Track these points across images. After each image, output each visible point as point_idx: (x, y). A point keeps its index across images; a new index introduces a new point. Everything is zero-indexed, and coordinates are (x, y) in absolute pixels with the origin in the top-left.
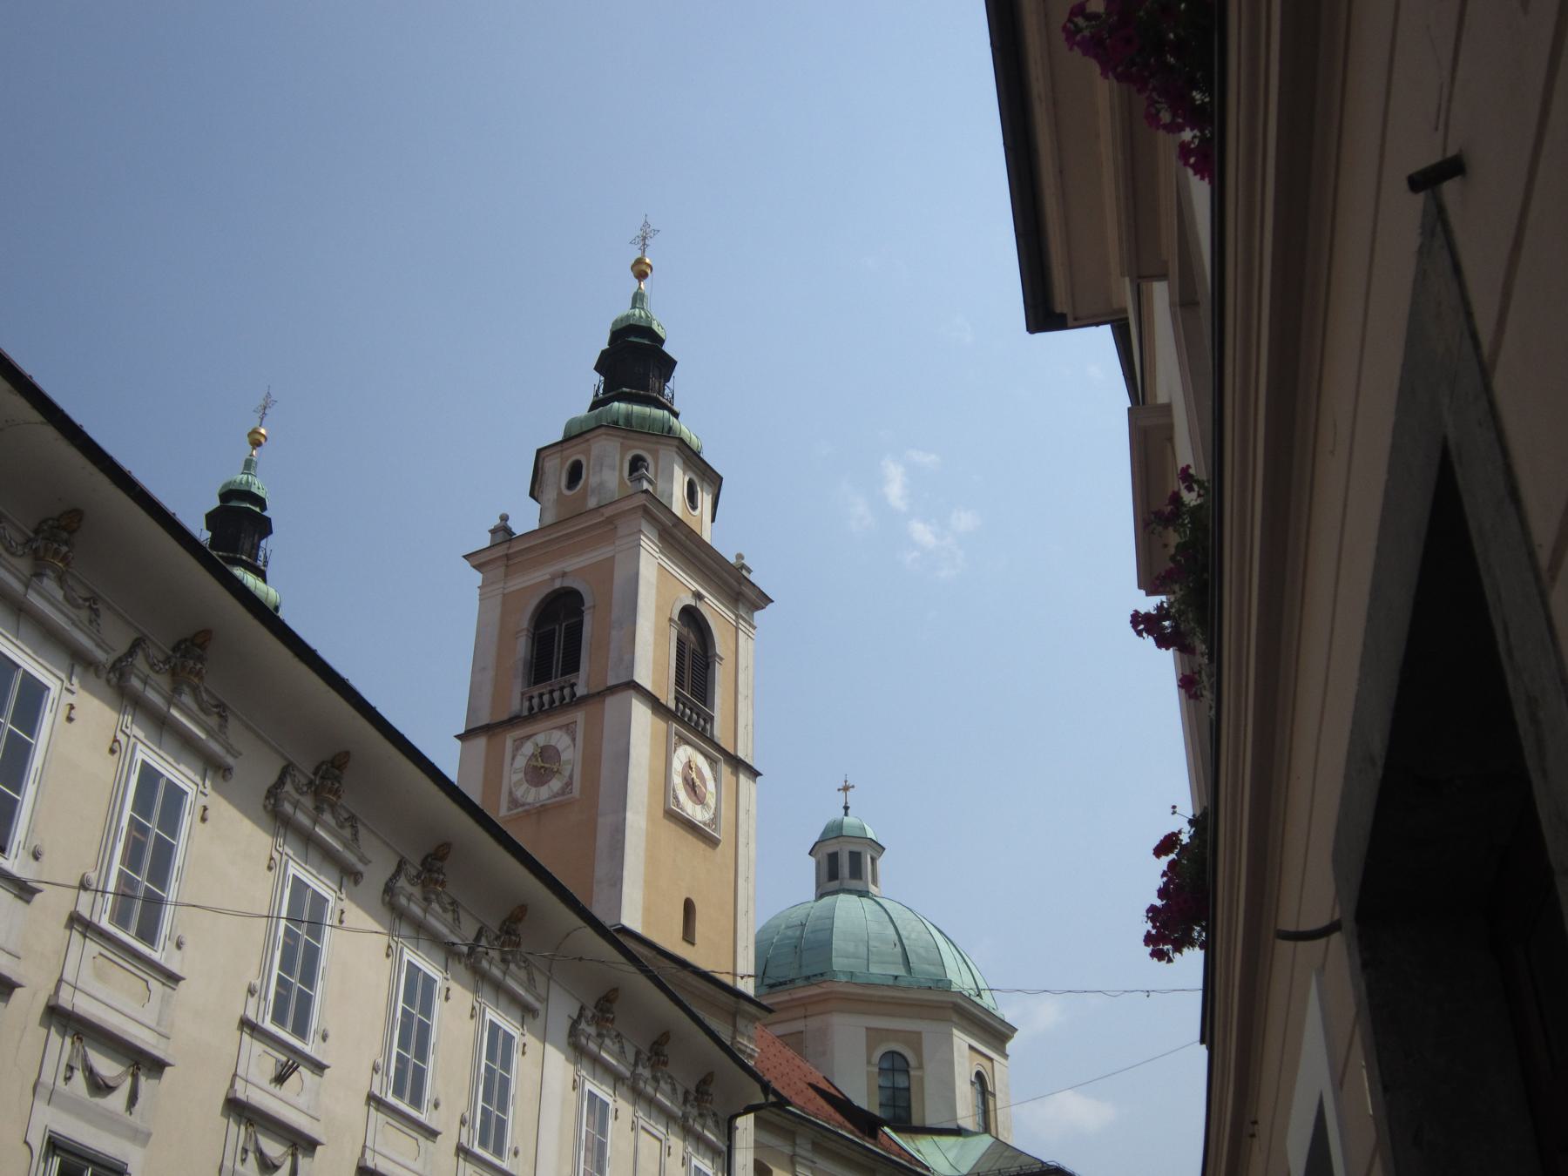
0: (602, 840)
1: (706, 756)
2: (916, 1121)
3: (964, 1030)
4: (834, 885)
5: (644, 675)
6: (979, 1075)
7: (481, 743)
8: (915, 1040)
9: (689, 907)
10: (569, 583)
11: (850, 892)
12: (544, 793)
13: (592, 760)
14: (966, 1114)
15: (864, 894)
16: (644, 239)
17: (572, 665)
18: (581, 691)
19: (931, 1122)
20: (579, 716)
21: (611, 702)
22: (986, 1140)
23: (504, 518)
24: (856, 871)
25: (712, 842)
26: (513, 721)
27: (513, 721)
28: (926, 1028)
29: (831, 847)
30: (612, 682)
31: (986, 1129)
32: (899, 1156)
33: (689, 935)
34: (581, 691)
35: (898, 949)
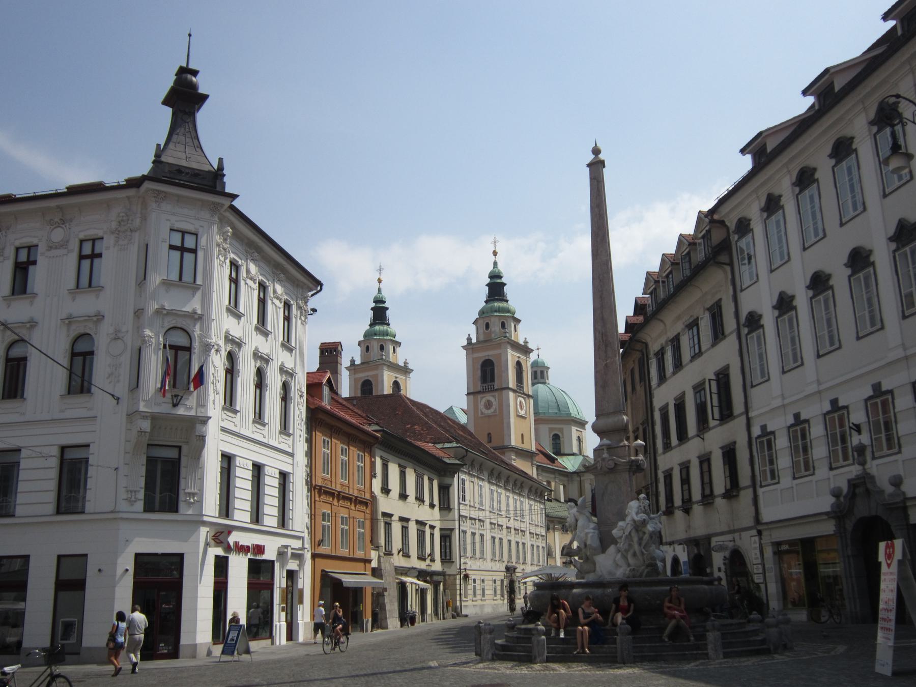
0: (505, 425)
1: (523, 398)
2: (562, 452)
3: (574, 426)
4: (536, 381)
5: (511, 386)
6: (579, 437)
7: (471, 397)
8: (561, 430)
9: (522, 435)
10: (490, 358)
11: (541, 383)
12: (490, 412)
13: (501, 405)
14: (575, 450)
15: (544, 383)
16: (495, 243)
17: (493, 380)
18: (496, 388)
19: (566, 452)
20: (496, 394)
21: (504, 392)
22: (580, 458)
23: (469, 335)
24: (542, 377)
25: (525, 418)
26: (479, 392)
27: (479, 392)
28: (565, 427)
29: (535, 369)
30: (504, 387)
31: (580, 453)
32: (560, 467)
33: (523, 442)
34: (496, 388)
35: (556, 404)
